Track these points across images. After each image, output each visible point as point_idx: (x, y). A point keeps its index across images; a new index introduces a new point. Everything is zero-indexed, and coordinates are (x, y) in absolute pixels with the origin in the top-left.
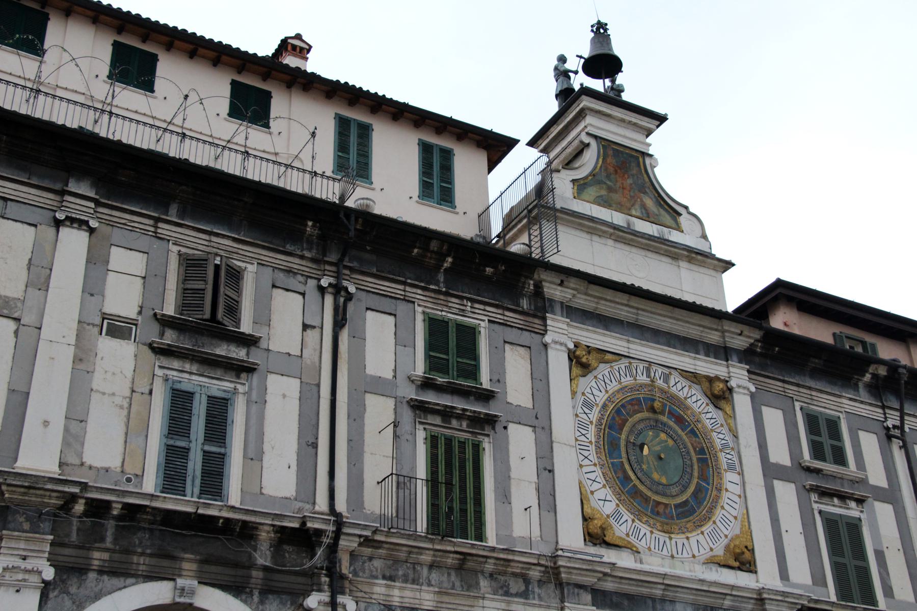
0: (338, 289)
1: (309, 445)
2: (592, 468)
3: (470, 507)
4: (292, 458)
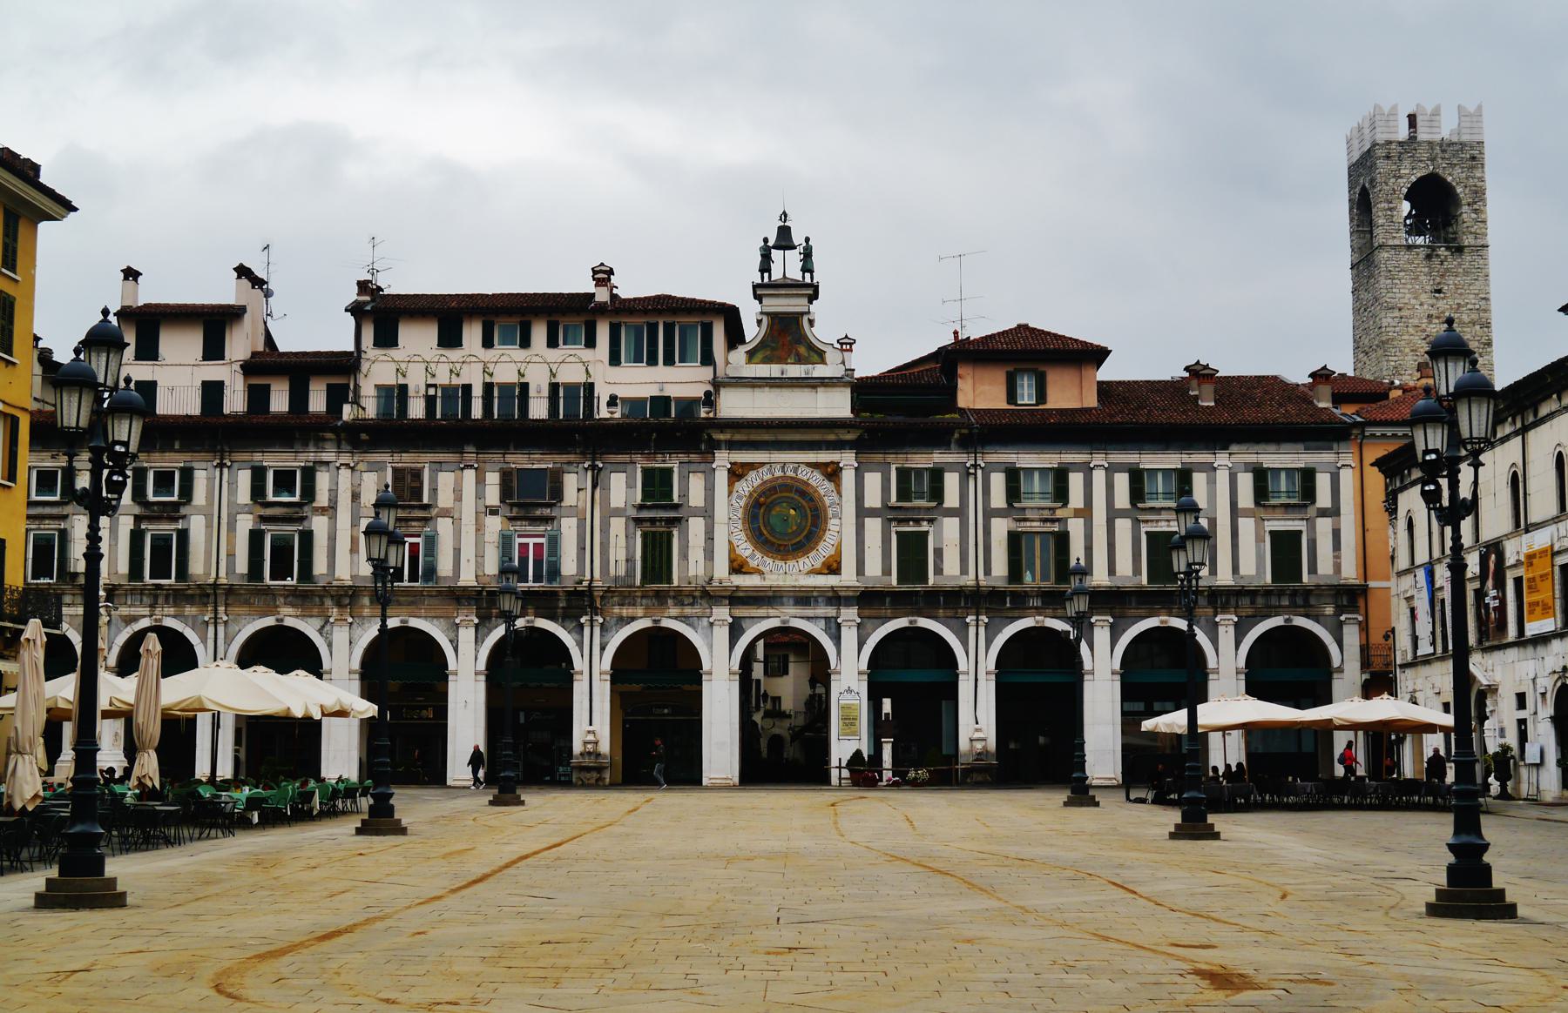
0: (593, 467)
1: (581, 549)
4: (575, 557)
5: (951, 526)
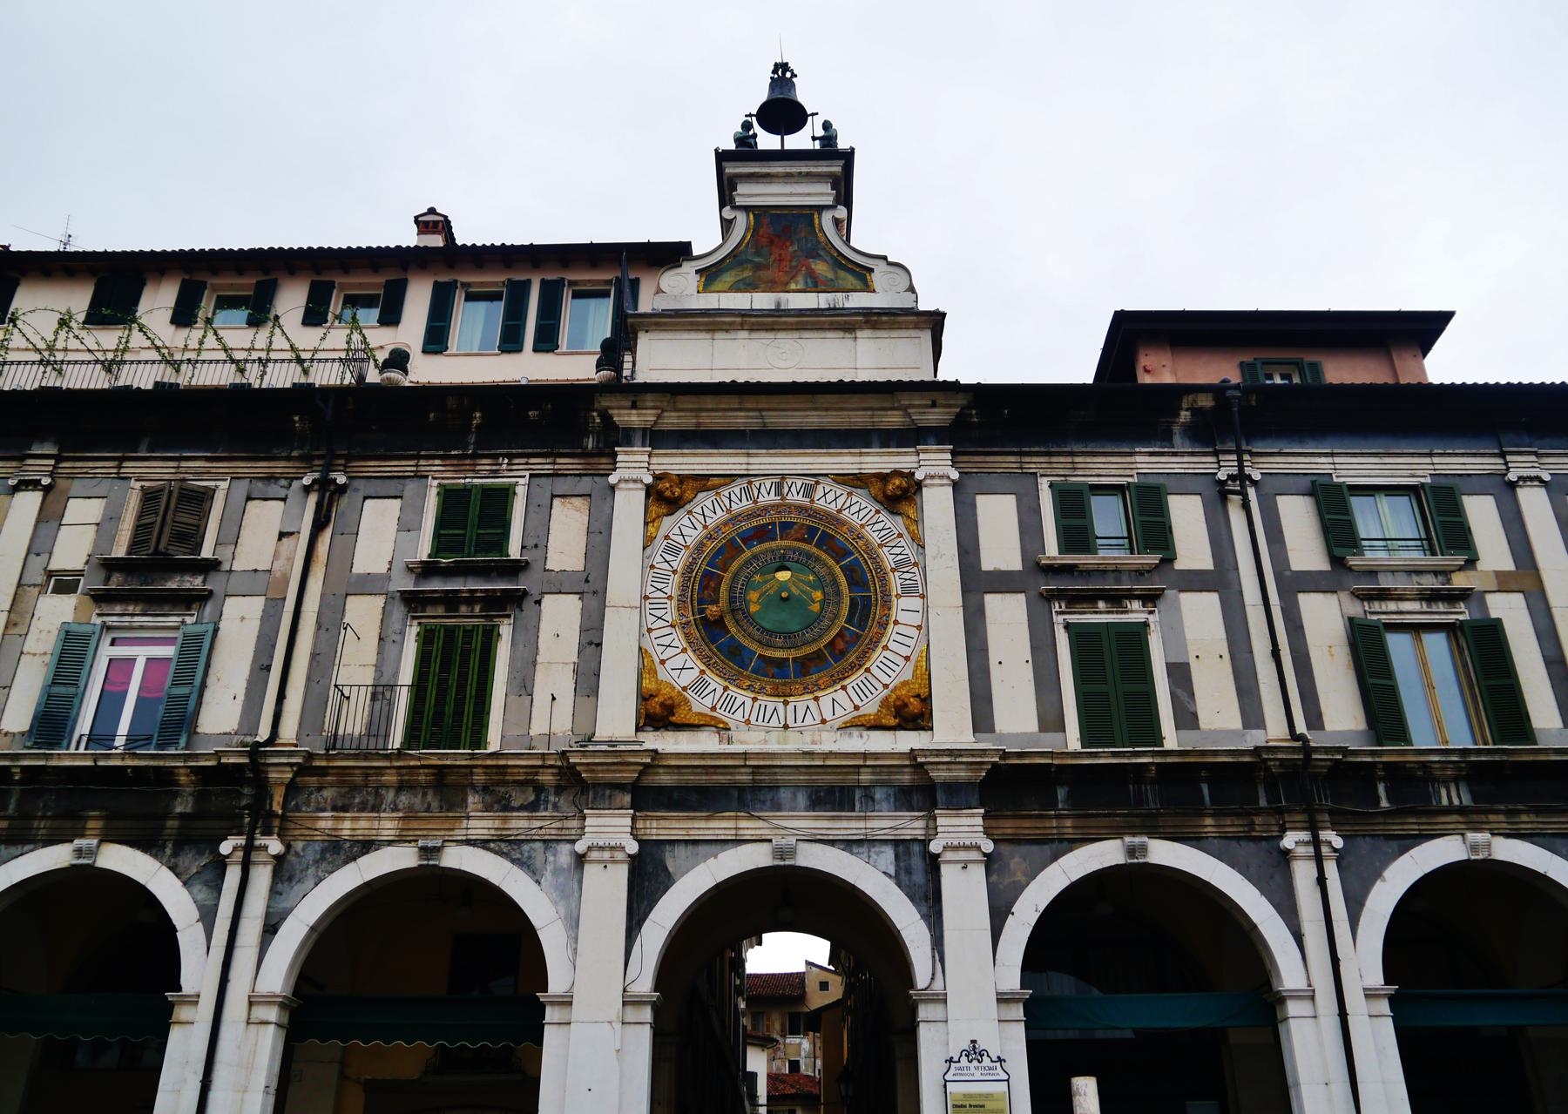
1: (261, 668)
2: (668, 630)
3: (469, 708)
5: (1200, 615)
